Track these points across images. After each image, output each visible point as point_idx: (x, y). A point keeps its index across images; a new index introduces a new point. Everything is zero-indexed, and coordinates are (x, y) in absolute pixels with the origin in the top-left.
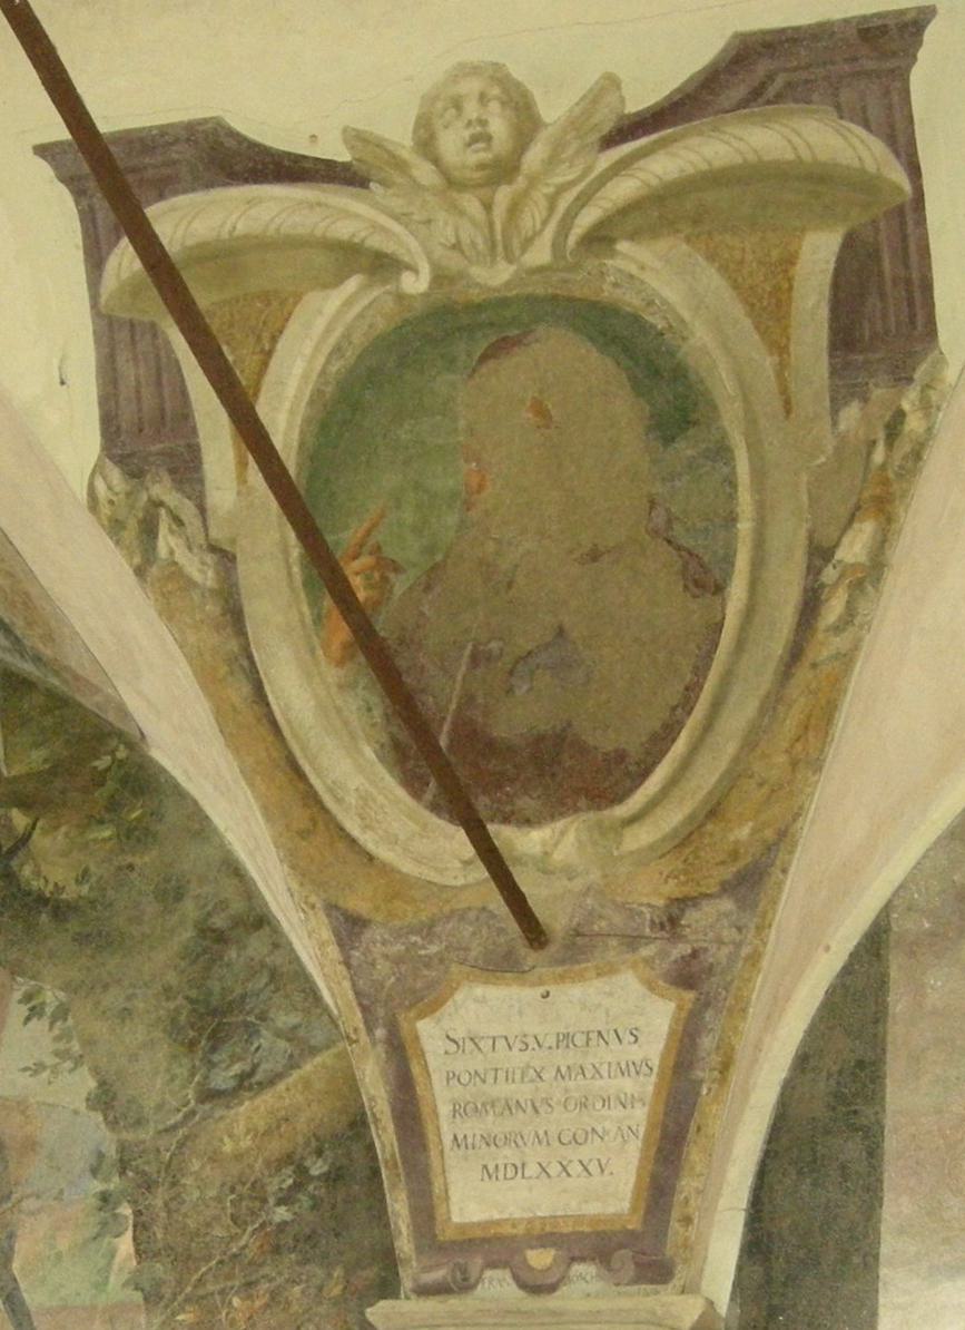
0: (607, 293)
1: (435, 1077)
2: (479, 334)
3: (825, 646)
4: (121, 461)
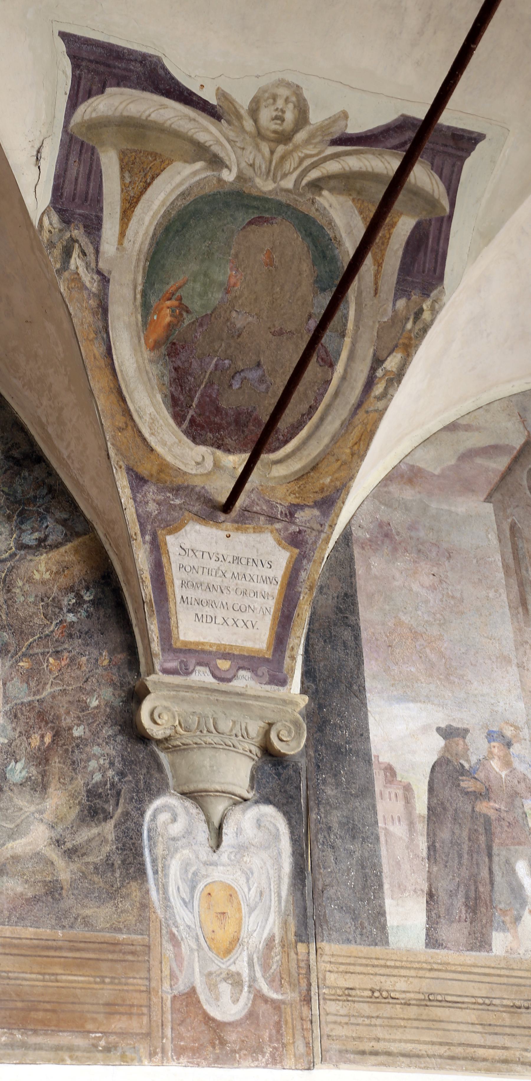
0: (313, 213)
1: (173, 565)
2: (250, 211)
3: (372, 404)
4: (61, 212)
